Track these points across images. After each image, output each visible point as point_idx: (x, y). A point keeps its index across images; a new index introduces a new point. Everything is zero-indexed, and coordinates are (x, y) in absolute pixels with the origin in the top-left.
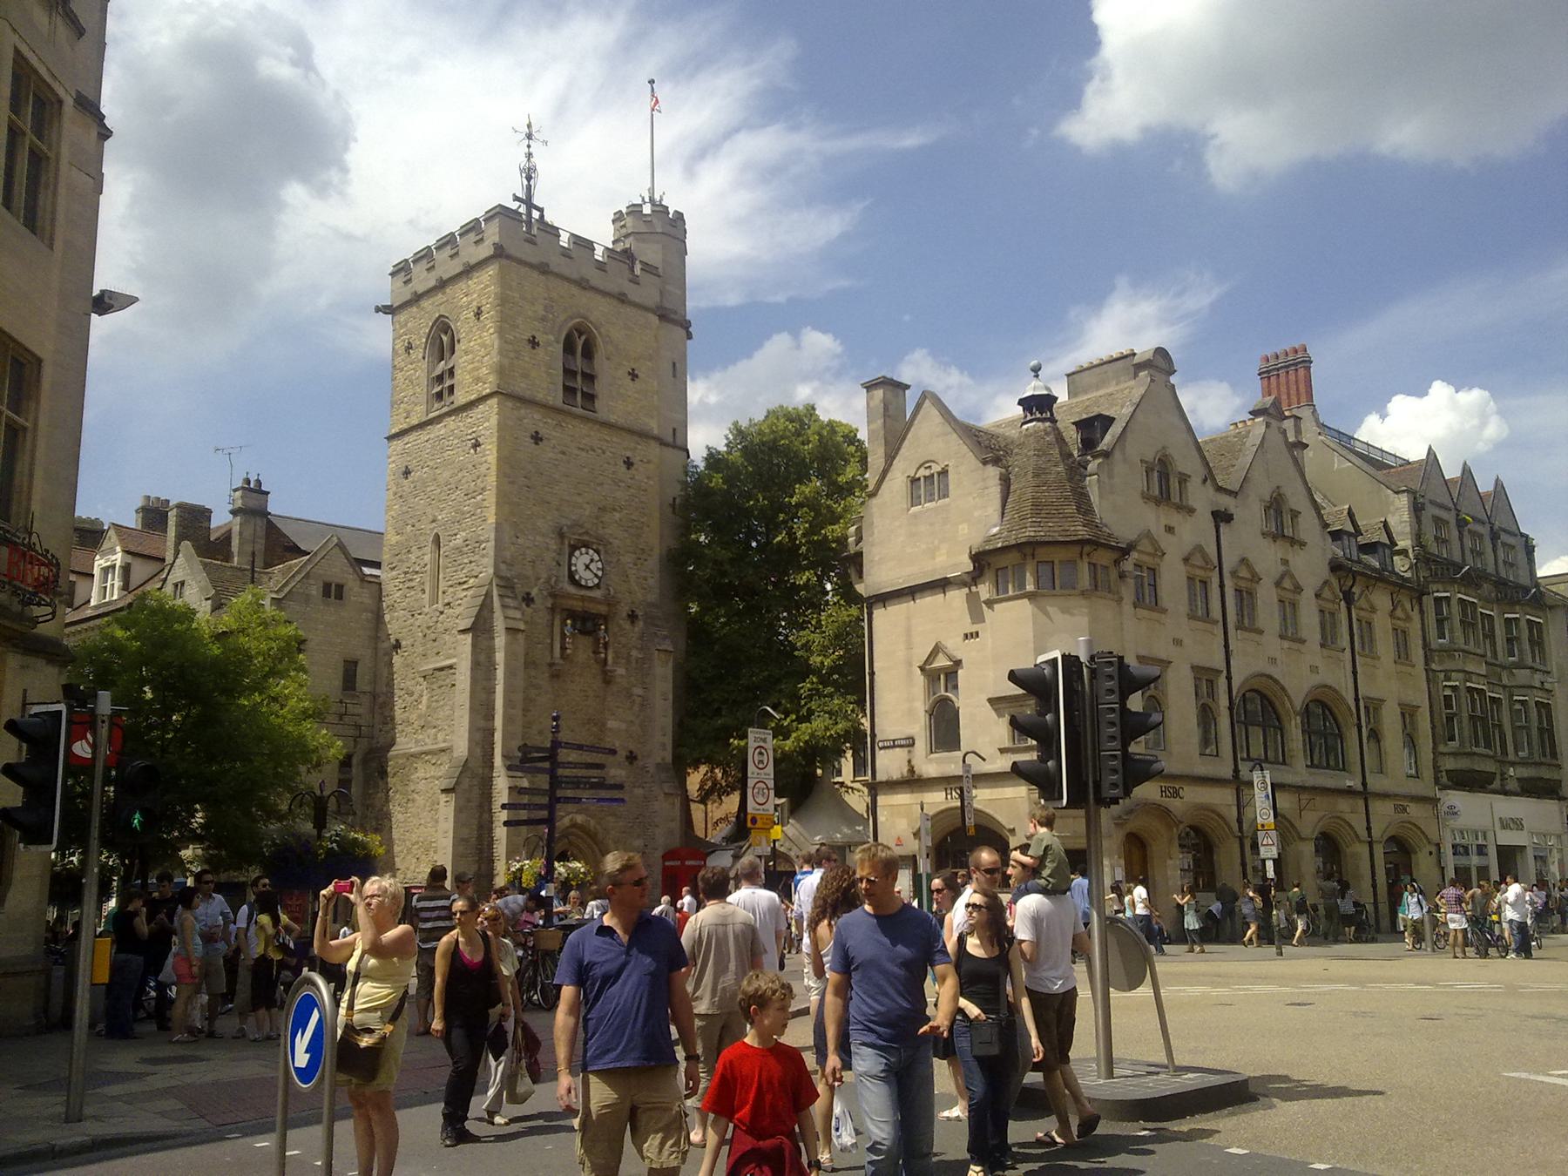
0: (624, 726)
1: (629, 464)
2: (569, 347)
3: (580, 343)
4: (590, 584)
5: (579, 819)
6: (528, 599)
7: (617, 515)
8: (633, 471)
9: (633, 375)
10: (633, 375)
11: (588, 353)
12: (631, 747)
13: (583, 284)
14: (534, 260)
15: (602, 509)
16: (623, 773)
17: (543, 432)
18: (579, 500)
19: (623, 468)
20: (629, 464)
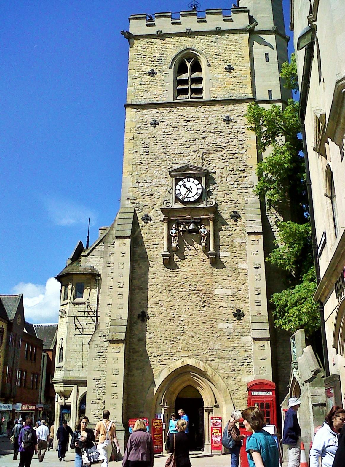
0: (230, 292)
1: (228, 120)
2: (181, 69)
3: (189, 65)
4: (192, 199)
5: (190, 362)
6: (147, 219)
7: (219, 154)
8: (231, 124)
9: (229, 69)
10: (229, 69)
11: (197, 67)
12: (238, 306)
13: (190, 34)
14: (155, 32)
15: (208, 153)
16: (231, 326)
17: (159, 119)
18: (188, 151)
19: (224, 124)
20: (228, 120)
